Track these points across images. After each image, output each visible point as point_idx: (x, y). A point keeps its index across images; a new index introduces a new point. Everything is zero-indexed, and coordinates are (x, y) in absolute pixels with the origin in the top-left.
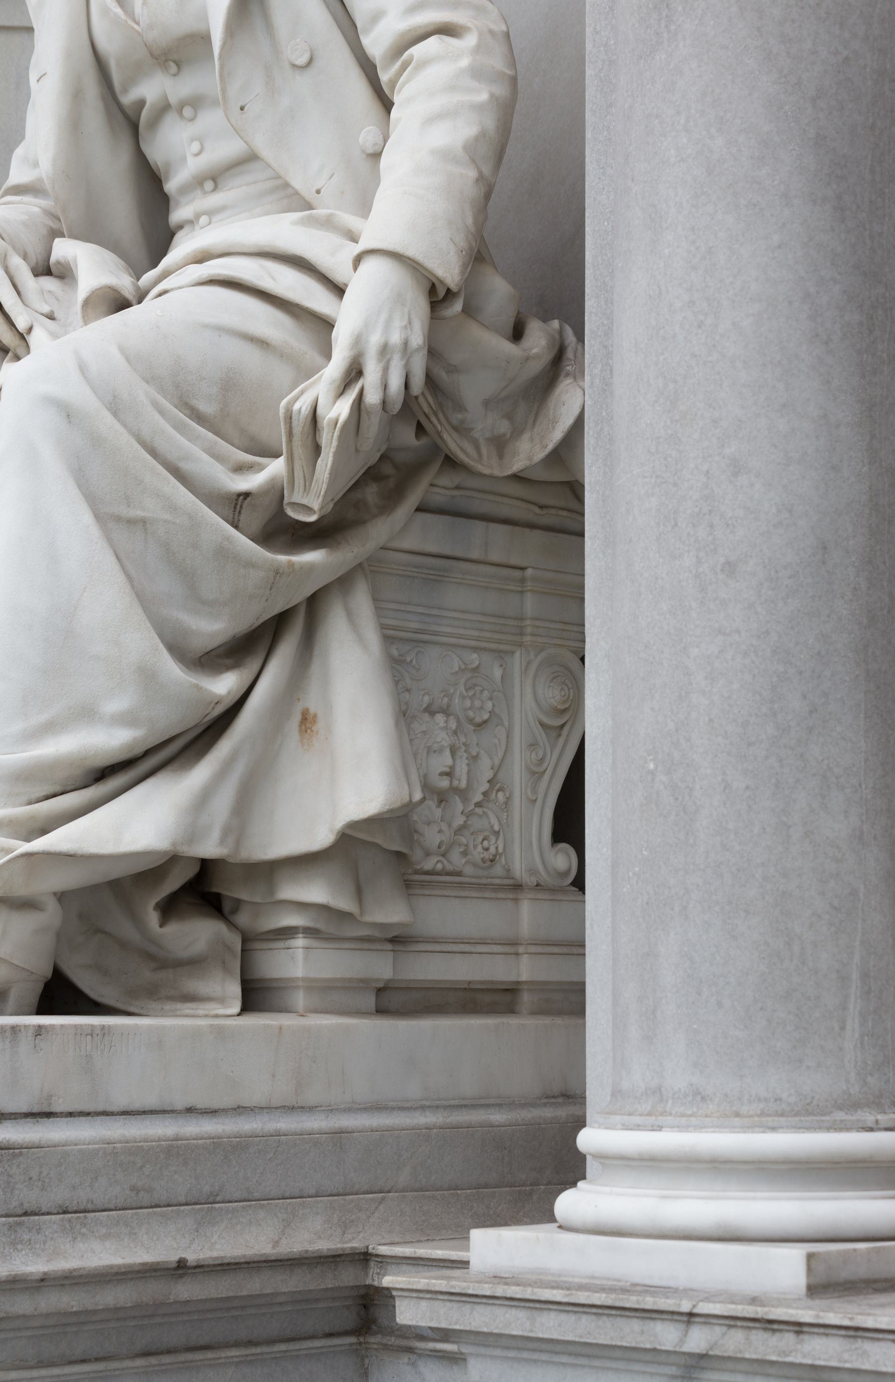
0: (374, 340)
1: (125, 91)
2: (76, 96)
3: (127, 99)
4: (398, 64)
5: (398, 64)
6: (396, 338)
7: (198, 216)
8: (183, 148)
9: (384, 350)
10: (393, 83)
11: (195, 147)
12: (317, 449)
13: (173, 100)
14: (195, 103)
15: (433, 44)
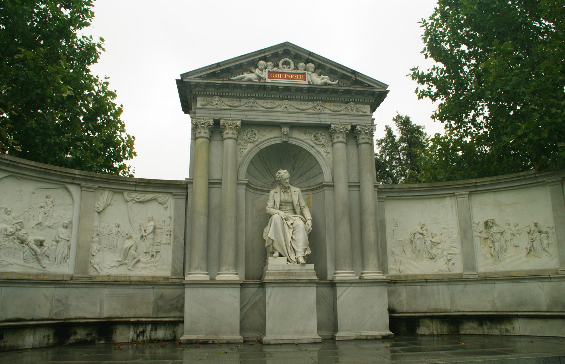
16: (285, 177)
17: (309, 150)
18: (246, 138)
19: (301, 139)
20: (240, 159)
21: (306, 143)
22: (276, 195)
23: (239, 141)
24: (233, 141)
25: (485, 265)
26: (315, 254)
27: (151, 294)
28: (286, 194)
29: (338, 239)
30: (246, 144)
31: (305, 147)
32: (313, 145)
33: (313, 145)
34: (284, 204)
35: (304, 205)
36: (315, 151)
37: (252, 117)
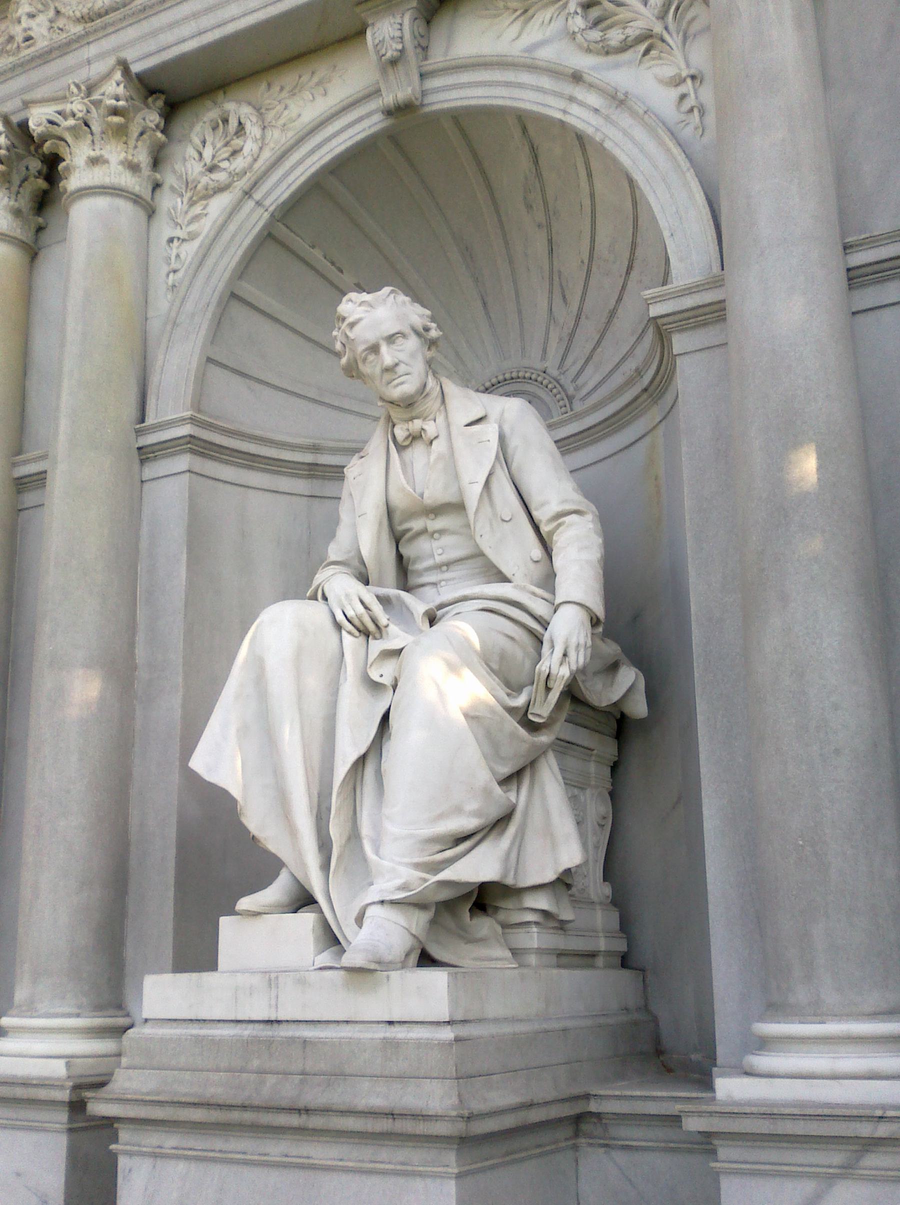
0: (573, 641)
1: (401, 523)
2: (380, 524)
3: (400, 528)
4: (555, 524)
5: (555, 524)
6: (582, 641)
7: (440, 581)
8: (428, 551)
9: (578, 646)
10: (551, 533)
11: (440, 551)
12: (548, 689)
13: (430, 529)
14: (442, 532)
15: (574, 517)
16: (363, 334)
17: (553, 108)
18: (194, 169)
20: (161, 303)
21: (532, 68)
23: (167, 201)
24: (125, 206)
28: (417, 453)
30: (197, 209)
31: (528, 100)
32: (583, 62)
33: (583, 62)
34: (416, 525)
35: (555, 507)
36: (593, 99)
37: (186, 30)
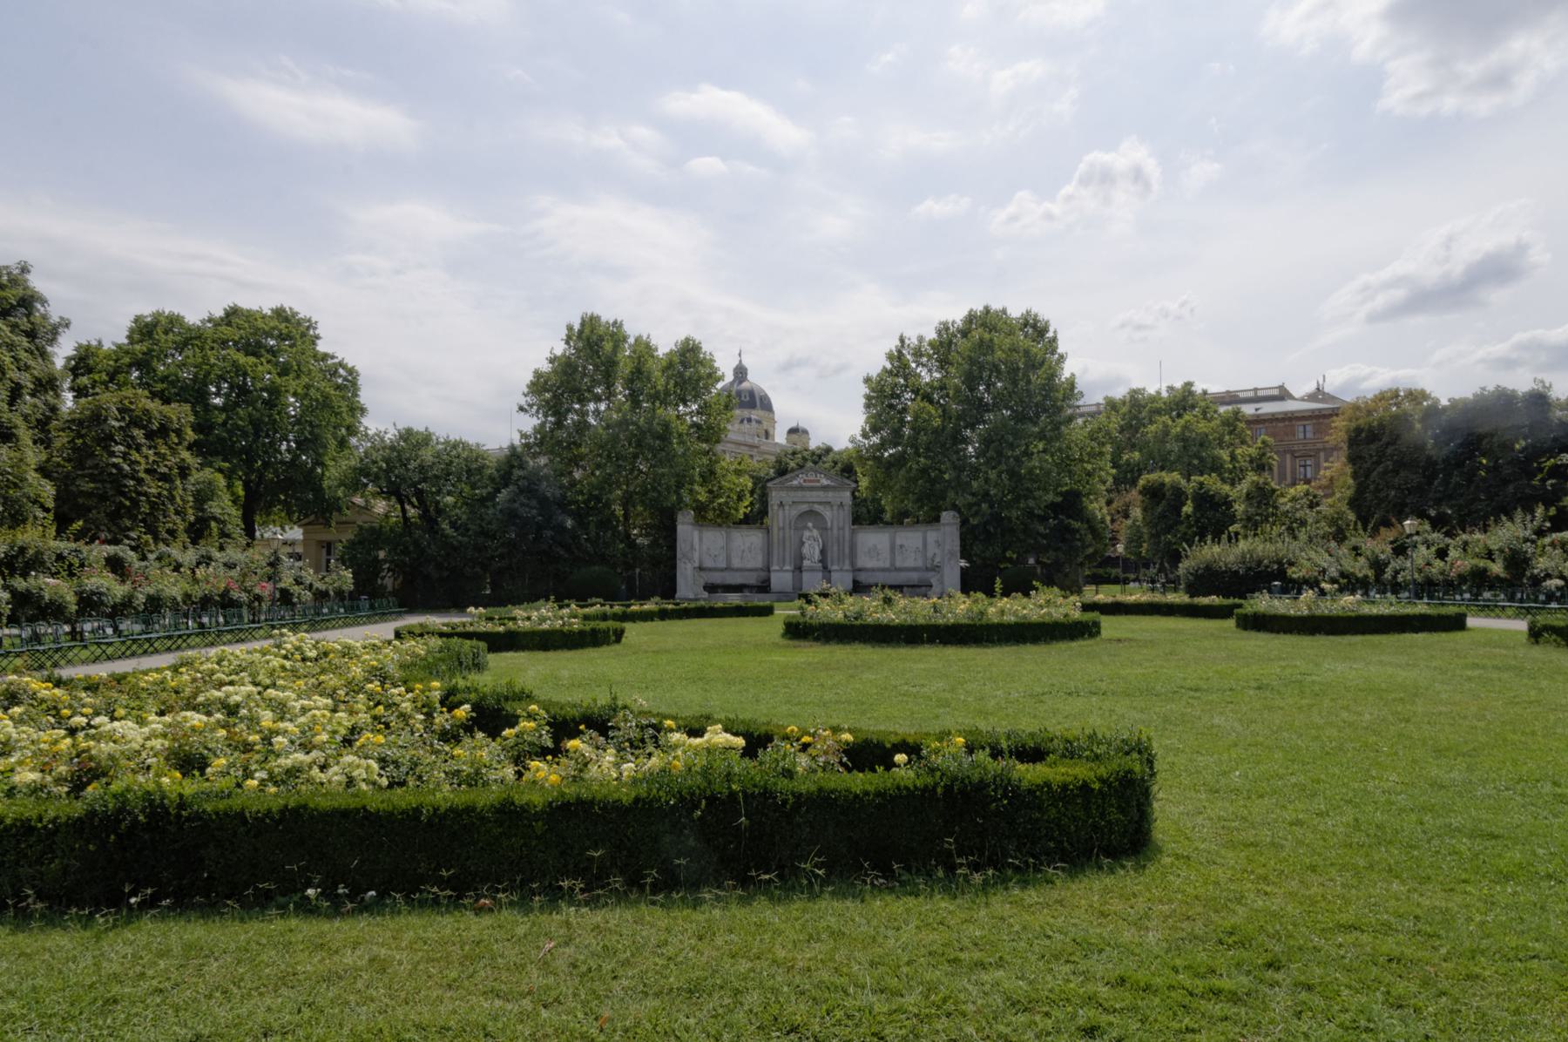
19: (817, 508)
22: (807, 534)
25: (898, 564)
26: (823, 561)
27: (755, 575)
29: (833, 552)
